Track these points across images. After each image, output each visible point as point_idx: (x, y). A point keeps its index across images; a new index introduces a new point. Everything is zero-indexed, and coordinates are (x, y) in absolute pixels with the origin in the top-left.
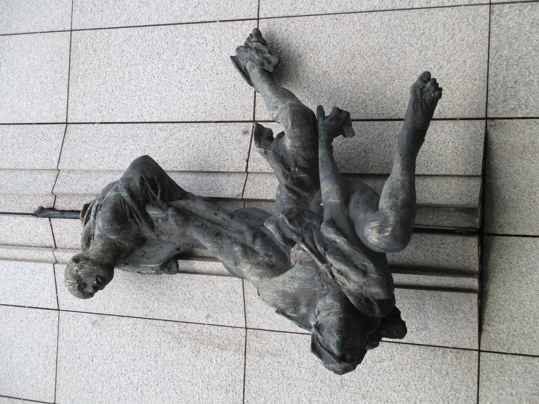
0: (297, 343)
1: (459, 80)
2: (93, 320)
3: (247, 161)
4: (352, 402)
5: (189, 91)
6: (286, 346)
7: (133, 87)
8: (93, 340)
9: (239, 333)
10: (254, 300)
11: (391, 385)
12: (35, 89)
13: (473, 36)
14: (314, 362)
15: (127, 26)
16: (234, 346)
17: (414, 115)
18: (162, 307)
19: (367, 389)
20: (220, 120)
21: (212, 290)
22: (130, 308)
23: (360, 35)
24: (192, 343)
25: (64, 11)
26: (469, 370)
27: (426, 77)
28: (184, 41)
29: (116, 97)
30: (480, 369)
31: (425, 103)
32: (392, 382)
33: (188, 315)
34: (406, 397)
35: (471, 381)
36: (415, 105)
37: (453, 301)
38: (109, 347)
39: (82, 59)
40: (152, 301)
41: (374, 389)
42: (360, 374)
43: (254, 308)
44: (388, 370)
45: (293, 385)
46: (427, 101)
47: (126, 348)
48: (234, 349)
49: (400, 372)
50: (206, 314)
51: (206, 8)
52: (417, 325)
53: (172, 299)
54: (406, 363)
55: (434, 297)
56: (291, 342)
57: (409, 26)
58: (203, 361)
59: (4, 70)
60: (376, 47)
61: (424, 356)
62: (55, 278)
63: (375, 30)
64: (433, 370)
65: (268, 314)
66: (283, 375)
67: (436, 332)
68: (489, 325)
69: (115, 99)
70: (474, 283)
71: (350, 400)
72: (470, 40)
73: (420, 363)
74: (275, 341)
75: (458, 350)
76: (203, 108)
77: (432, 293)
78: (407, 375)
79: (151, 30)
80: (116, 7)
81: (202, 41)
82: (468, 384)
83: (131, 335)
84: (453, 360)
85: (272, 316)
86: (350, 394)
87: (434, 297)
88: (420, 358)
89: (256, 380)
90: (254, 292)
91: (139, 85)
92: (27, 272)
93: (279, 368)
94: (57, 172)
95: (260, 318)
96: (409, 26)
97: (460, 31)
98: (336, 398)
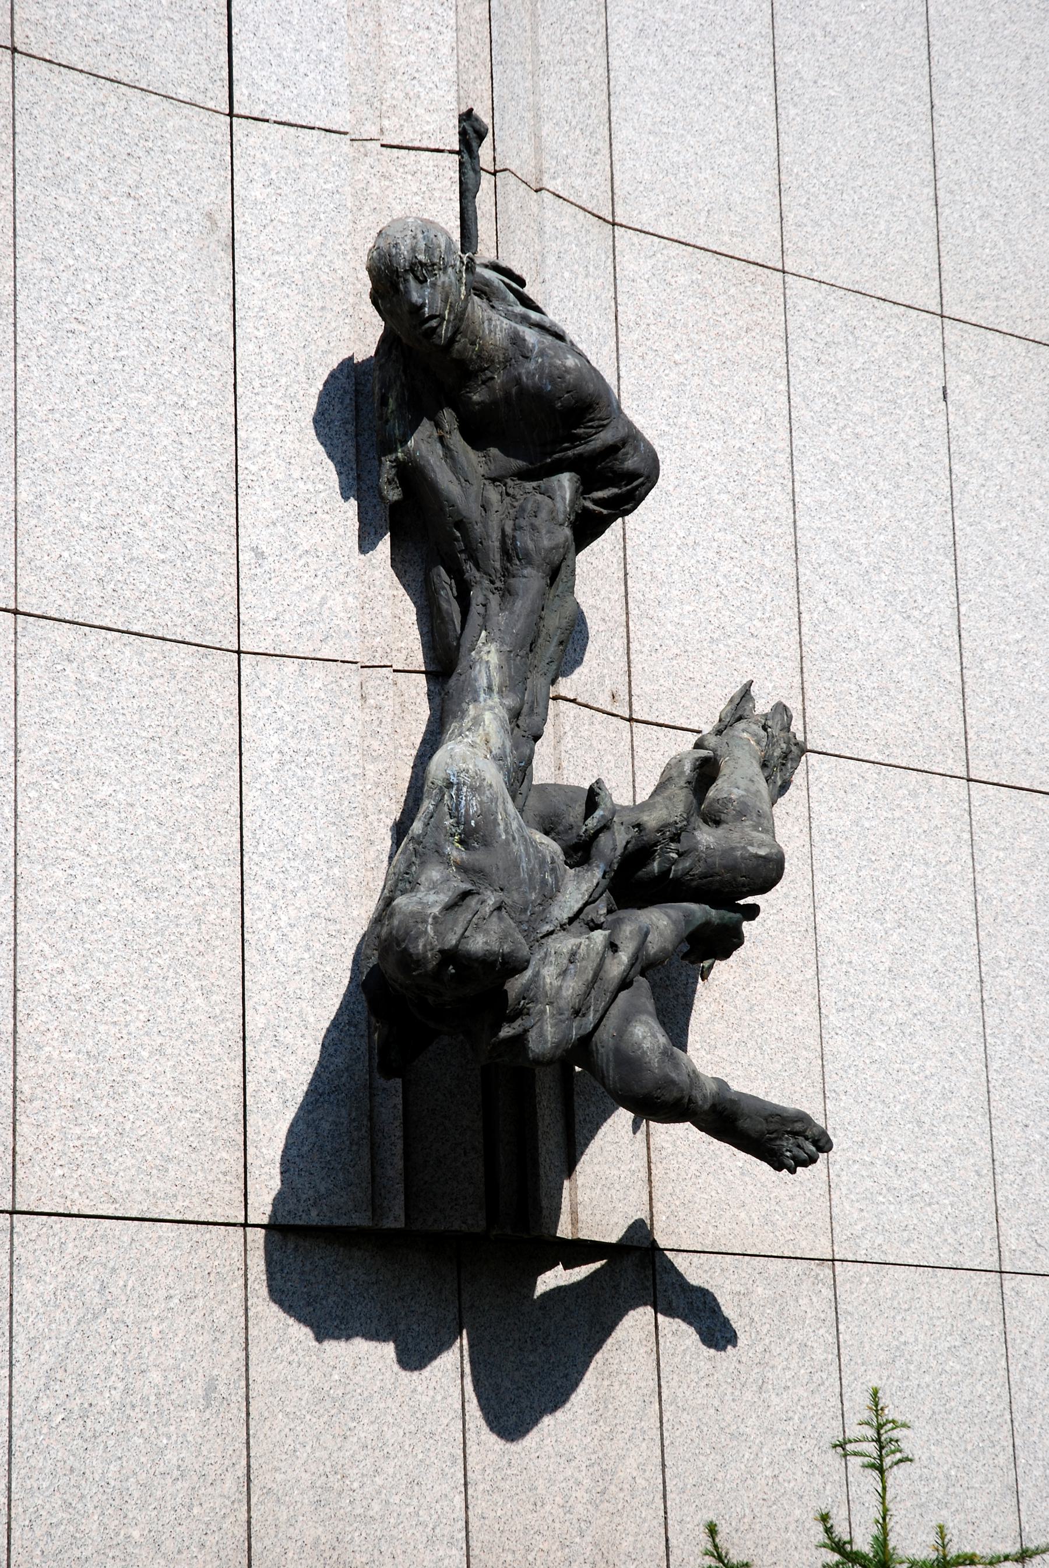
0: (221, 783)
1: (713, 1193)
2: (217, 216)
3: (574, 701)
4: (115, 914)
5: (681, 564)
6: (211, 754)
7: (684, 419)
8: (175, 208)
9: (228, 632)
10: (310, 684)
11: (160, 1013)
12: (676, 146)
13: (784, 1223)
14: (186, 822)
15: (793, 421)
16: (199, 614)
17: (760, 1116)
18: (269, 429)
19: (144, 952)
20: (631, 635)
21: (325, 575)
22: (256, 333)
23: (782, 981)
24: (195, 497)
25: (819, 259)
26: (207, 1200)
27: (823, 1143)
28: (769, 565)
29: (667, 372)
30: (210, 1227)
31: (776, 1139)
32: (165, 1017)
33: (255, 498)
34: (139, 1049)
35: (185, 1204)
36: (776, 1119)
37: (351, 1170)
38: (162, 253)
39: (733, 291)
40: (280, 403)
41: (146, 970)
42: (173, 938)
43: (291, 681)
44: (189, 1007)
45: (133, 762)
46: (778, 1142)
47: (168, 306)
48: (192, 612)
49: (187, 1037)
50: (264, 549)
51: (823, 626)
52: (289, 1084)
53: (293, 461)
54: (207, 1052)
55: (358, 1129)
56: (222, 769)
57: (798, 1089)
58: (160, 524)
59: (710, 63)
60: (763, 1014)
61: (224, 1097)
62: (313, 128)
63: (790, 1016)
64: (198, 1115)
65: (280, 714)
66: (152, 738)
67: (277, 1127)
68: (296, 1249)
69: (662, 369)
70: (392, 1218)
71: (117, 908)
72: (777, 1217)
73: (209, 1086)
74: (220, 724)
75: (243, 1176)
76: (652, 597)
77: (365, 1122)
78: (183, 1054)
79: (785, 482)
80: (825, 400)
81: (768, 608)
82: (180, 1197)
83: (196, 324)
84: (222, 1163)
85: (275, 725)
86: (130, 909)
87: (358, 1129)
88: (219, 1087)
89: (134, 665)
90: (329, 687)
91: (689, 436)
92: (323, 45)
93: (167, 729)
94: (534, 186)
95: (266, 692)
96: (798, 1089)
97: (792, 1198)
98: (119, 871)
